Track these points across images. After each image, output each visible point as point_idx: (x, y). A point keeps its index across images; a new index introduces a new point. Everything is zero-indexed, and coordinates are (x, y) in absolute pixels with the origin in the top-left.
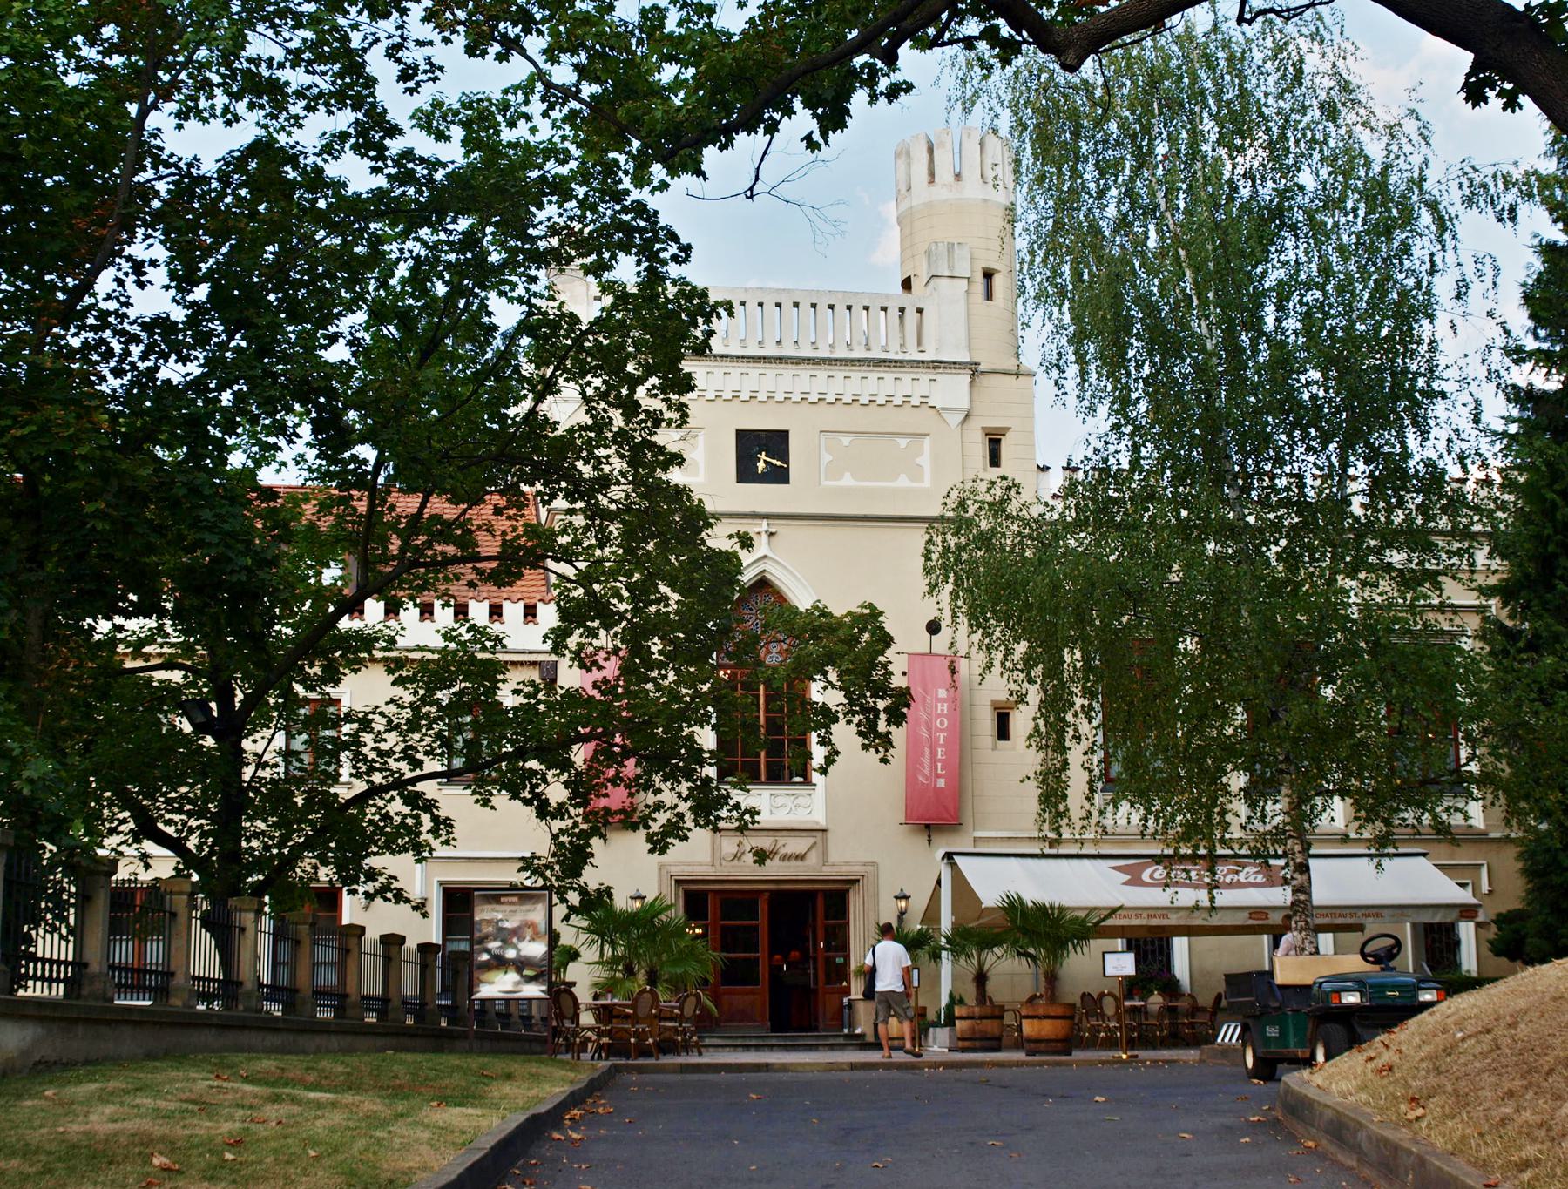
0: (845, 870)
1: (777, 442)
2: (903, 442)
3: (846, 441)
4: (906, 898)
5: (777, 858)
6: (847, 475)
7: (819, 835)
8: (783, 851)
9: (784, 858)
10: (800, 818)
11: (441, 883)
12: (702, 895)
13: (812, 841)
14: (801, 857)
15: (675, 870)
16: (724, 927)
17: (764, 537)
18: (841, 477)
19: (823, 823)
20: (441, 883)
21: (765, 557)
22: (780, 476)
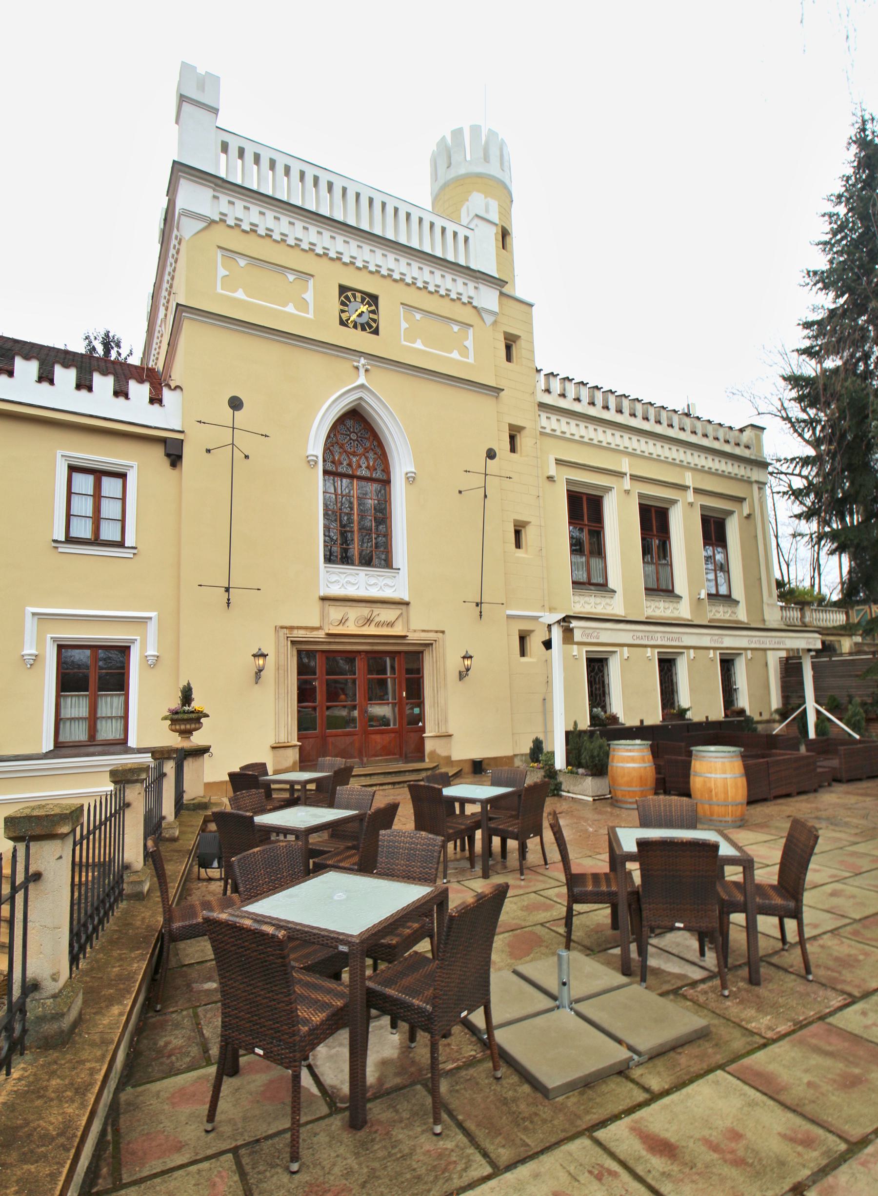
0: (424, 635)
1: (372, 299)
2: (456, 328)
3: (418, 316)
4: (471, 657)
5: (373, 624)
7: (404, 607)
8: (377, 619)
9: (378, 625)
10: (388, 593)
11: (54, 640)
12: (311, 654)
13: (398, 612)
14: (391, 624)
16: (327, 680)
17: (362, 371)
18: (414, 342)
19: (407, 599)
20: (54, 640)
21: (362, 386)
22: (372, 327)
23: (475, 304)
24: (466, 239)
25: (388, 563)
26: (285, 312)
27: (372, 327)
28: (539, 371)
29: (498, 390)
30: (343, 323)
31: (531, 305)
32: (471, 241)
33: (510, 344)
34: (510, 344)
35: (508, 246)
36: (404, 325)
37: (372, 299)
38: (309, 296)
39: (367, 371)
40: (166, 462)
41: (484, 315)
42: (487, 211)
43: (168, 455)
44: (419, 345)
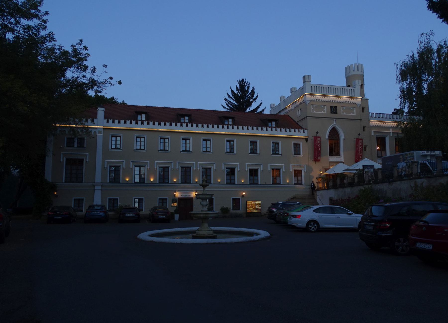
1: (336, 107)
2: (352, 108)
6: (345, 113)
15: (325, 168)
17: (335, 121)
21: (335, 124)
22: (336, 112)
23: (356, 103)
24: (354, 90)
25: (340, 155)
26: (322, 113)
27: (336, 112)
28: (370, 113)
29: (361, 120)
30: (331, 113)
31: (368, 100)
32: (355, 90)
33: (363, 109)
34: (363, 109)
35: (363, 87)
36: (342, 110)
37: (336, 107)
38: (325, 109)
39: (336, 121)
40: (306, 141)
41: (358, 105)
42: (358, 83)
43: (306, 140)
44: (345, 114)
